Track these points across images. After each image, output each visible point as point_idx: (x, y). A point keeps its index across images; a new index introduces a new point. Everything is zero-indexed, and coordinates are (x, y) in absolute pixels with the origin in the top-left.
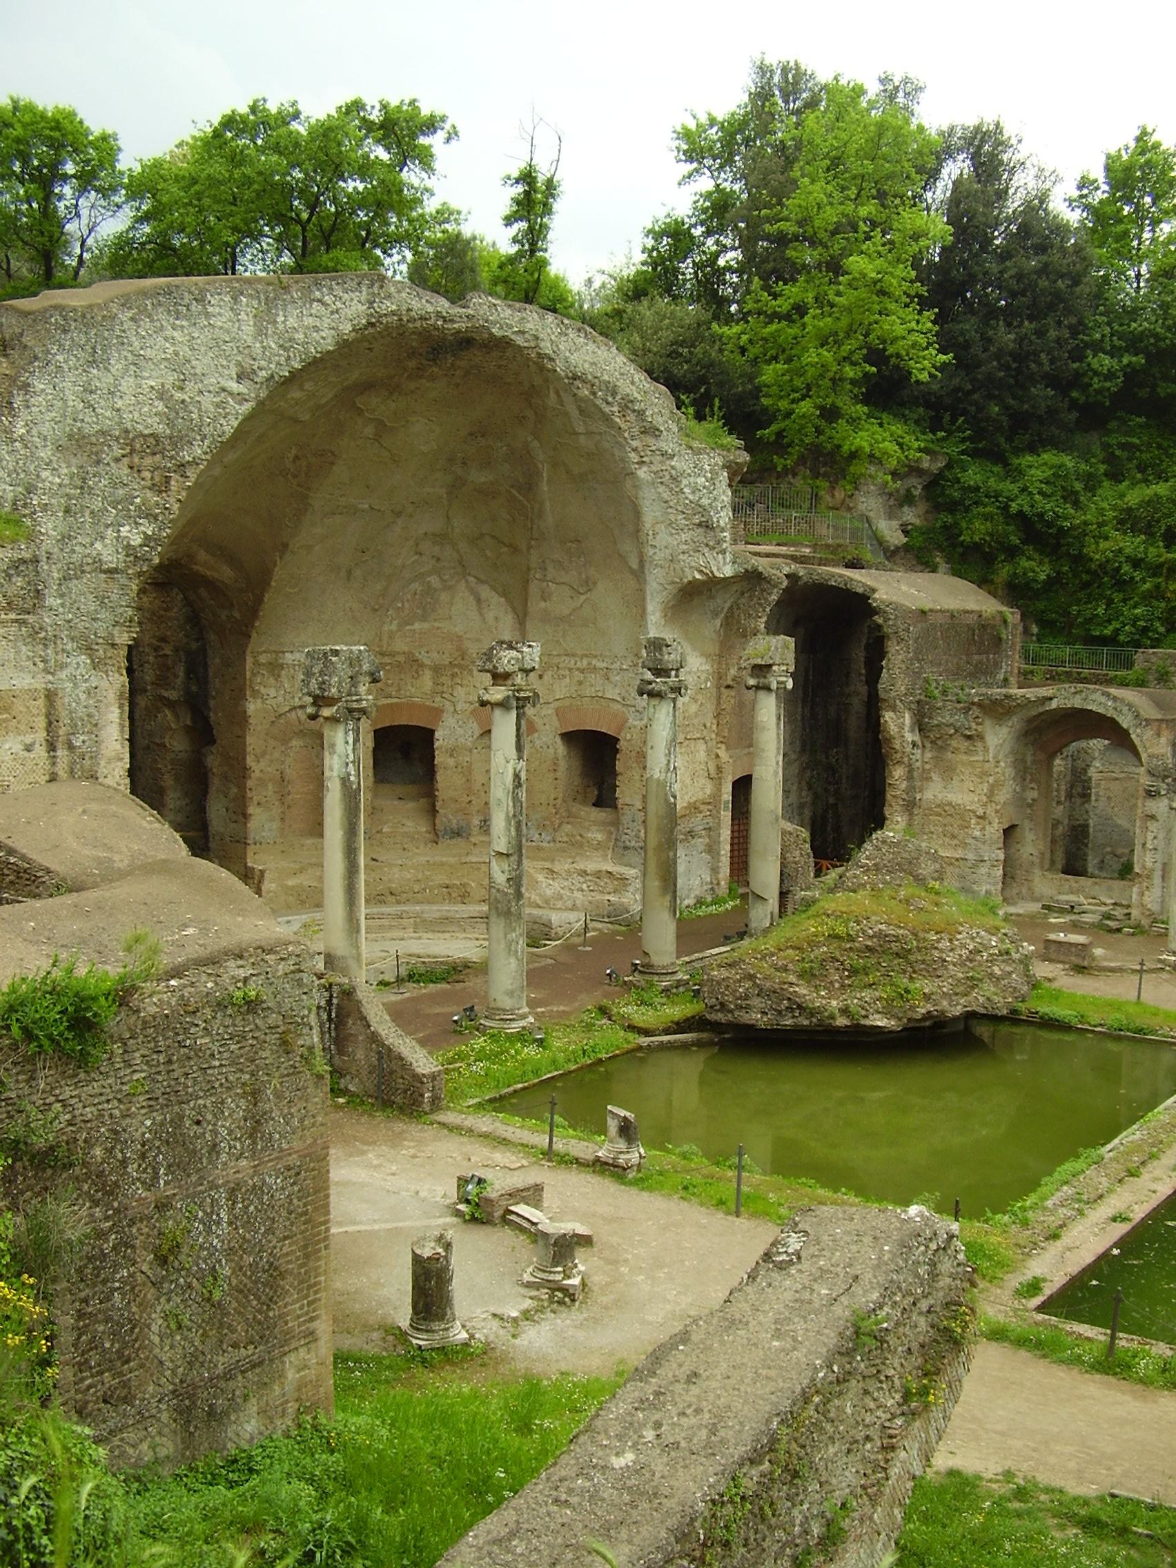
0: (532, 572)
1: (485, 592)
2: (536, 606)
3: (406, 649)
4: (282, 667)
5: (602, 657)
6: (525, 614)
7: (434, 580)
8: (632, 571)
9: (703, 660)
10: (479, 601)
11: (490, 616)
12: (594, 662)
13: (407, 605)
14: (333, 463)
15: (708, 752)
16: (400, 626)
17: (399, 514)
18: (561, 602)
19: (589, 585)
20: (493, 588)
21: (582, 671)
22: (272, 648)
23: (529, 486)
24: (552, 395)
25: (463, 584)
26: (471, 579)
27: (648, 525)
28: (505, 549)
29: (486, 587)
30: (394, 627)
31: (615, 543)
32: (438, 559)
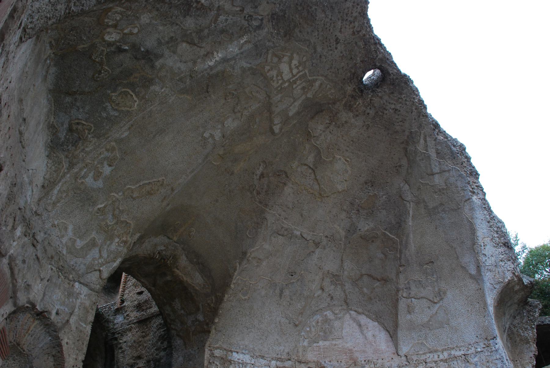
0: (401, 292)
1: (363, 319)
2: (404, 318)
3: (315, 359)
4: (230, 362)
5: (458, 348)
6: (396, 326)
7: (329, 313)
8: (471, 276)
10: (360, 326)
11: (369, 335)
12: (453, 352)
13: (313, 330)
14: (285, 184)
16: (309, 343)
17: (317, 245)
18: (422, 313)
19: (441, 295)
20: (368, 316)
21: (445, 361)
22: (225, 346)
23: (398, 226)
24: (422, 141)
25: (348, 316)
26: (352, 312)
27: (480, 239)
28: (378, 284)
29: (364, 317)
30: (306, 343)
31: (458, 258)
32: (332, 298)
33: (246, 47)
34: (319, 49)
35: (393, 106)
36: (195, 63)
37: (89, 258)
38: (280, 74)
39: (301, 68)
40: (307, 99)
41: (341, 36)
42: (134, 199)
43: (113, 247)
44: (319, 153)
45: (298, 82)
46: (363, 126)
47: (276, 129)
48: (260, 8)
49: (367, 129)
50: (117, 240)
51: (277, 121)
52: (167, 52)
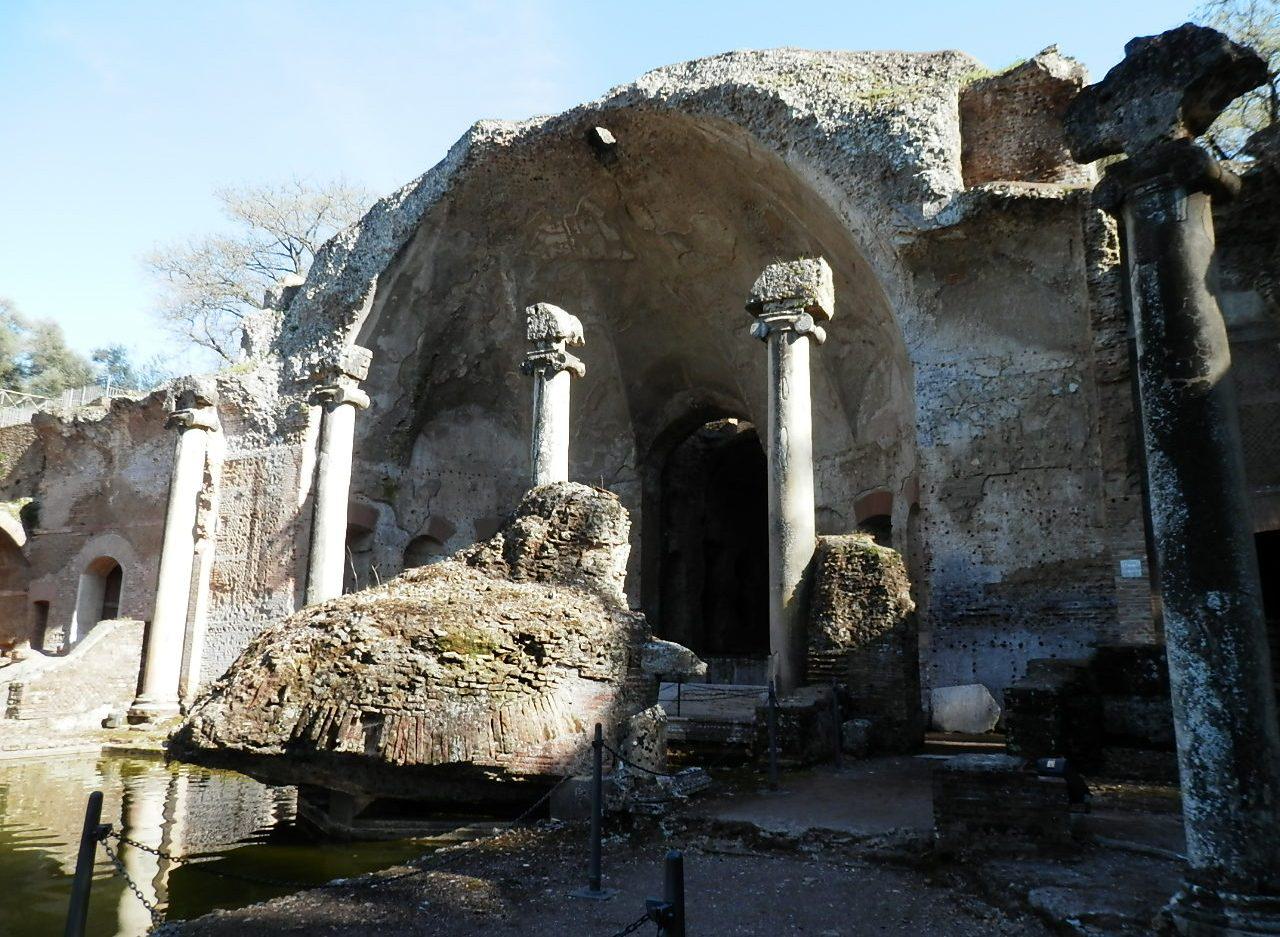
9: (1058, 355)
15: (1090, 488)
27: (836, 210)
33: (513, 276)
34: (542, 199)
35: (646, 136)
36: (509, 321)
37: (607, 465)
38: (556, 245)
39: (559, 223)
40: (605, 218)
41: (533, 174)
42: (596, 409)
43: (619, 445)
44: (676, 235)
45: (576, 227)
46: (663, 176)
47: (627, 256)
48: (479, 256)
49: (669, 173)
50: (617, 440)
51: (617, 254)
52: (493, 337)
